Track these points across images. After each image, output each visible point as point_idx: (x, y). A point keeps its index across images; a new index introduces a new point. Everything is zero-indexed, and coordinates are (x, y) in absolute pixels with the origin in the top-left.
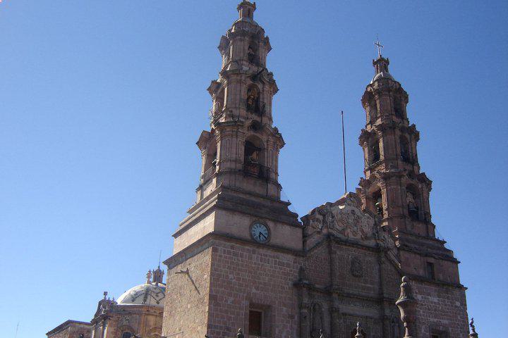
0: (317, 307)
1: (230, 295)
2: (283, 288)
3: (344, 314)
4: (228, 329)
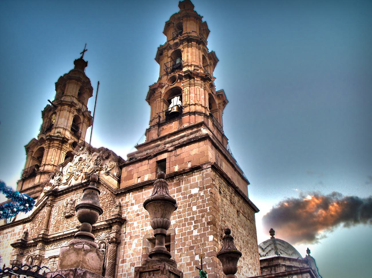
3: (51, 258)
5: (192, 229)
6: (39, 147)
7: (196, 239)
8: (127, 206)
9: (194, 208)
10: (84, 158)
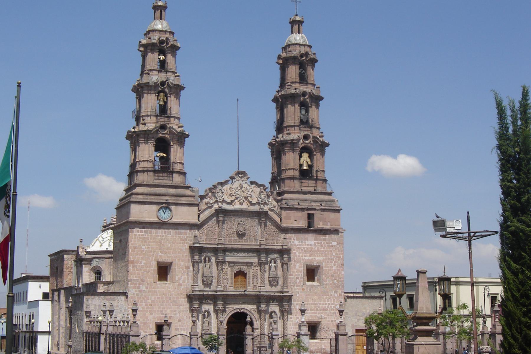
0: (207, 259)
1: (142, 259)
4: (143, 281)
5: (333, 265)
7: (335, 271)
8: (290, 239)
9: (334, 254)
10: (244, 185)
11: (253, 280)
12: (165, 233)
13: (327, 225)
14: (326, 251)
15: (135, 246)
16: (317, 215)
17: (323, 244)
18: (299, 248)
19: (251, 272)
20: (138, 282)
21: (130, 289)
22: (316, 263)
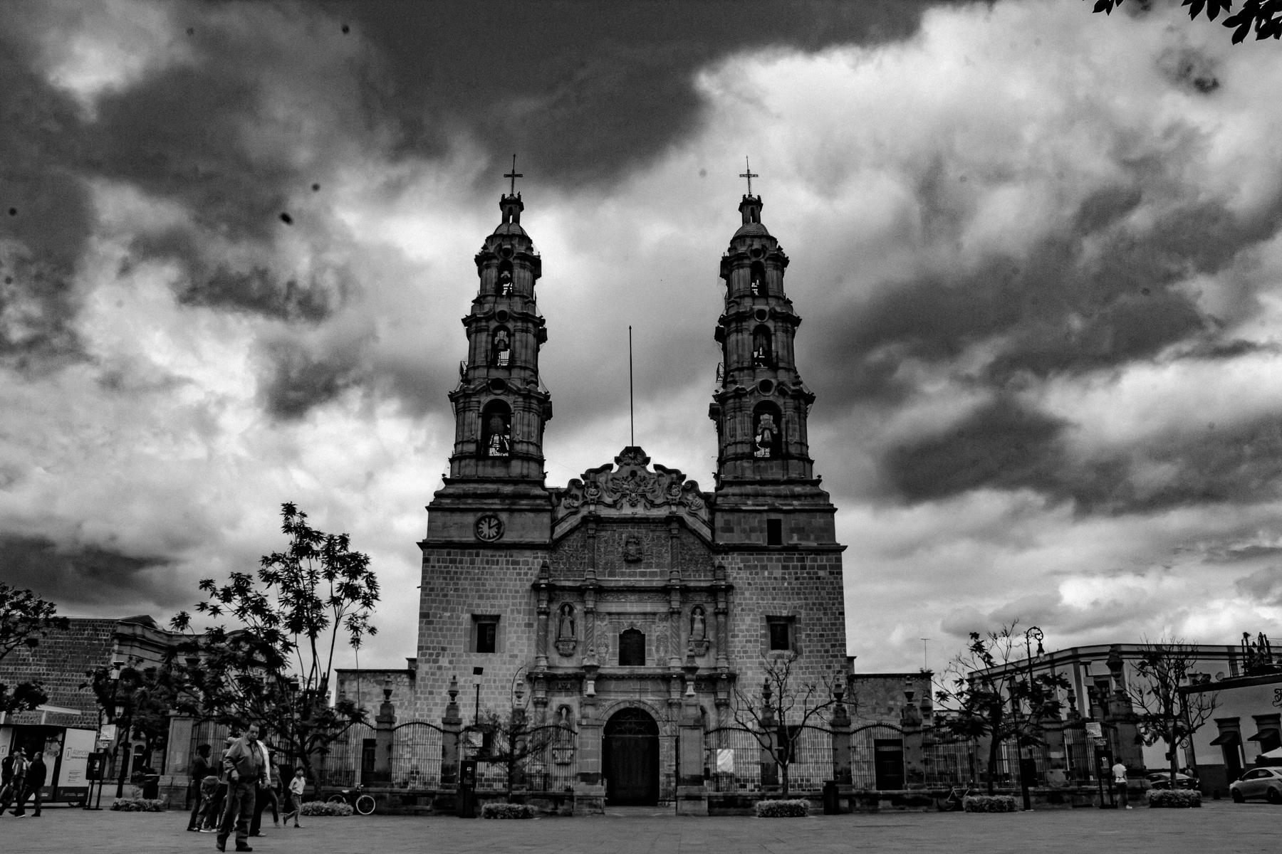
0: (567, 609)
1: (445, 610)
2: (517, 592)
3: (610, 614)
4: (444, 649)
6: (492, 397)
10: (639, 473)
11: (658, 648)
12: (487, 563)
13: (808, 539)
14: (806, 588)
15: (431, 586)
16: (787, 523)
17: (799, 575)
18: (749, 584)
19: (654, 632)
20: (435, 652)
21: (420, 664)
22: (786, 611)
